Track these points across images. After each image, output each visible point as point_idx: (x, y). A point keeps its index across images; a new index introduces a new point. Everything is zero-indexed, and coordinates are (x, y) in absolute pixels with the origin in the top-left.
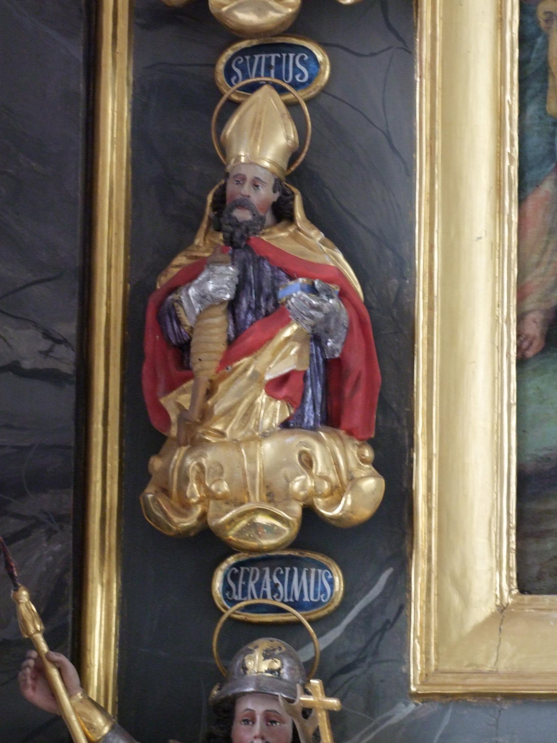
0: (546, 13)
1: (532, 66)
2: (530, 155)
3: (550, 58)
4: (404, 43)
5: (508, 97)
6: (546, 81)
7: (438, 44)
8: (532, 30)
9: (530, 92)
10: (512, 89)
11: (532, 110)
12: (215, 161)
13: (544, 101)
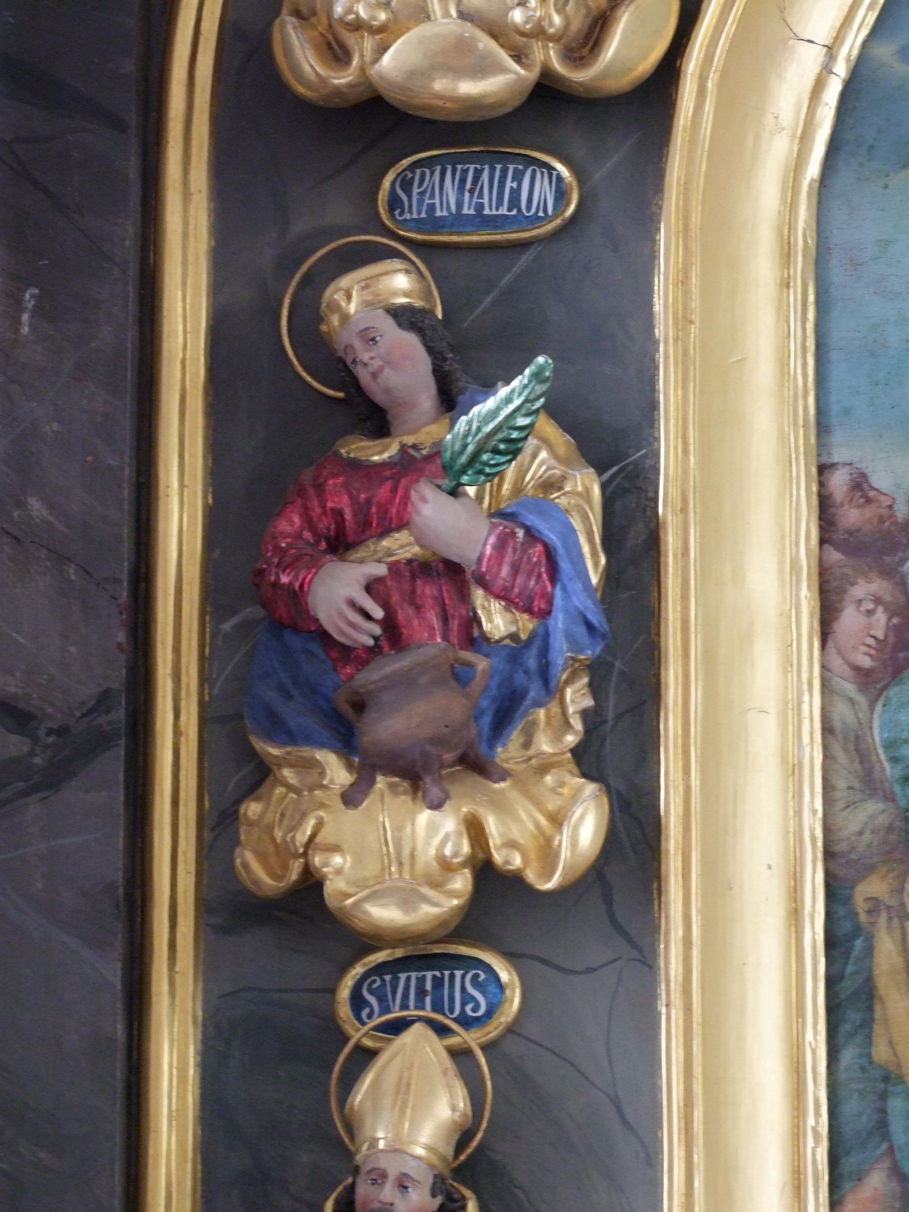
0: (867, 899)
1: (847, 986)
2: (847, 1130)
3: (876, 972)
4: (641, 951)
5: (809, 1036)
6: (870, 1008)
7: (696, 952)
8: (846, 927)
9: (845, 1028)
10: (815, 1024)
11: (848, 1056)
12: (337, 1147)
13: (869, 1041)
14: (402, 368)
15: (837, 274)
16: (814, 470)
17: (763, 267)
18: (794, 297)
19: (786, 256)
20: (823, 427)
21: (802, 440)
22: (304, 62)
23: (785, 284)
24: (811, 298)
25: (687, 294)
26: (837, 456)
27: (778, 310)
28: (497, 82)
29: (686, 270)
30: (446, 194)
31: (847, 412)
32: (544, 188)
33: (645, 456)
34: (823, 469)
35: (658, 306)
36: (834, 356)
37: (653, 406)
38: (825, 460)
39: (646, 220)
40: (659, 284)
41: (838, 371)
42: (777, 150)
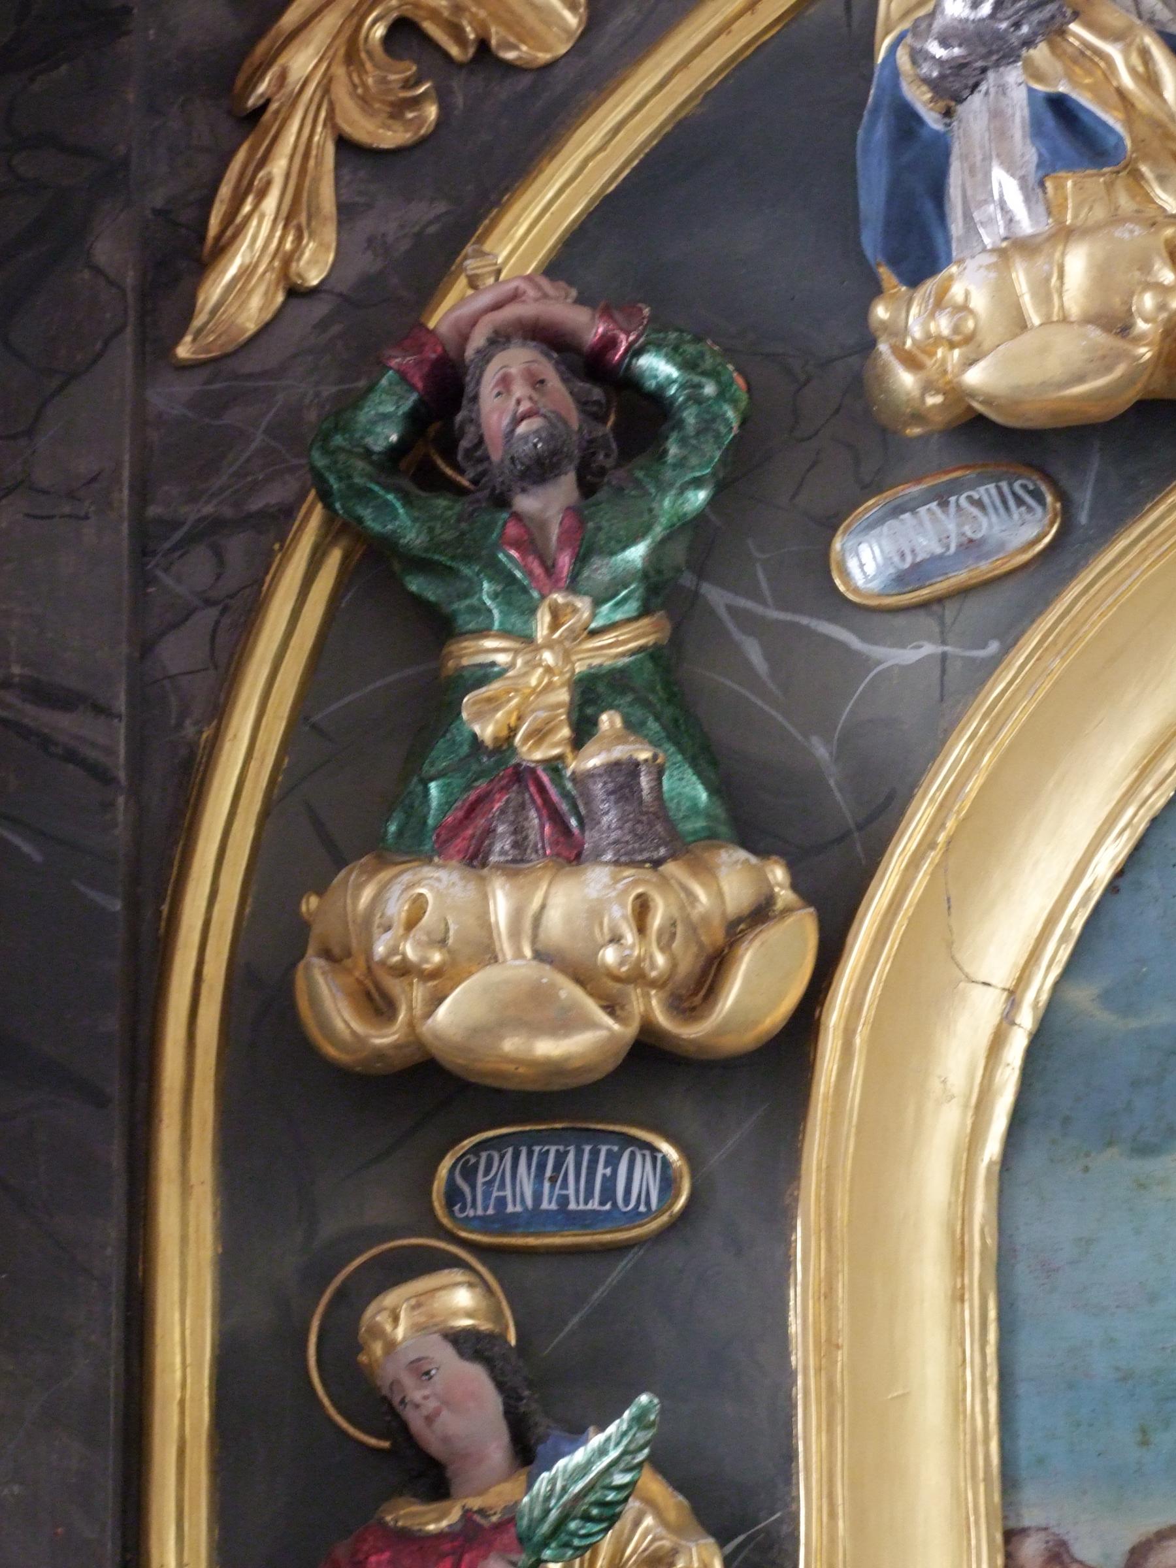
14: (464, 1410)
15: (1025, 1281)
16: (999, 1537)
17: (929, 1275)
18: (969, 1313)
19: (959, 1259)
20: (1010, 1480)
21: (982, 1498)
22: (335, 1016)
23: (958, 1296)
24: (992, 1314)
25: (831, 1310)
26: (1030, 1517)
27: (950, 1329)
28: (583, 1041)
29: (830, 1277)
30: (521, 1185)
31: (1041, 1461)
32: (648, 1174)
33: (780, 1521)
34: (1011, 1536)
35: (795, 1326)
36: (1023, 1388)
37: (790, 1456)
38: (1012, 1524)
39: (778, 1216)
40: (795, 1296)
41: (1028, 1409)
42: (945, 1125)
